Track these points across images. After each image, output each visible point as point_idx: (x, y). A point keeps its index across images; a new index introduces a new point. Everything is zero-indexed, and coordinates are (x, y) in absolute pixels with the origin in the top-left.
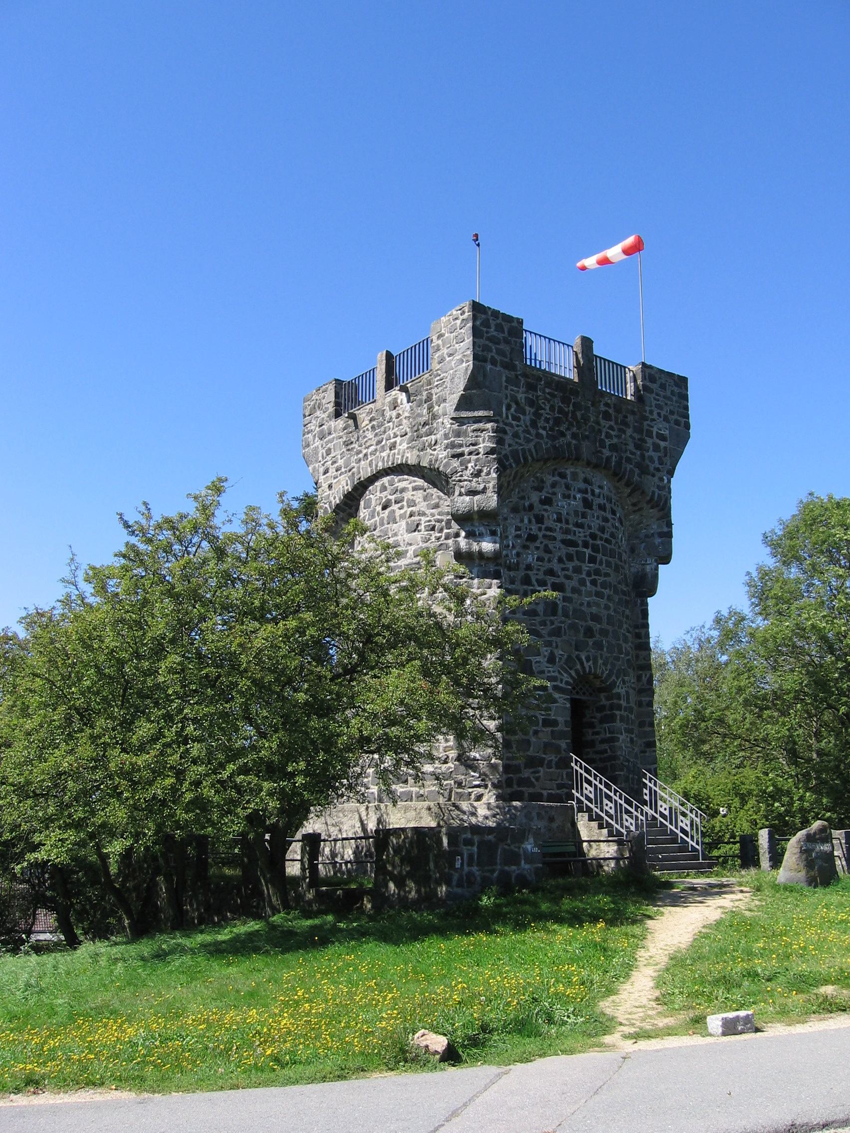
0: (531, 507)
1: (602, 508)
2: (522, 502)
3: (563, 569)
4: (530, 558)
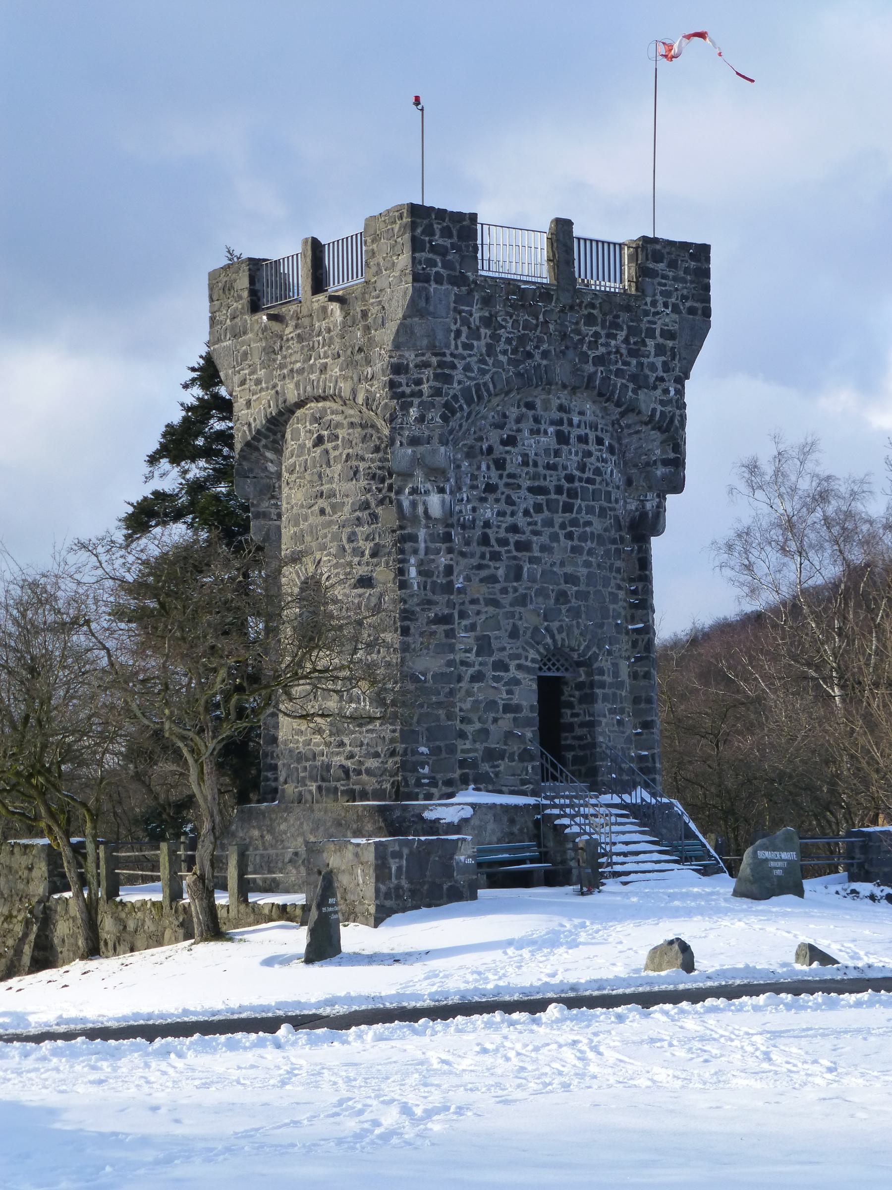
0: (490, 450)
1: (583, 439)
2: (479, 444)
3: (529, 524)
4: (488, 512)
